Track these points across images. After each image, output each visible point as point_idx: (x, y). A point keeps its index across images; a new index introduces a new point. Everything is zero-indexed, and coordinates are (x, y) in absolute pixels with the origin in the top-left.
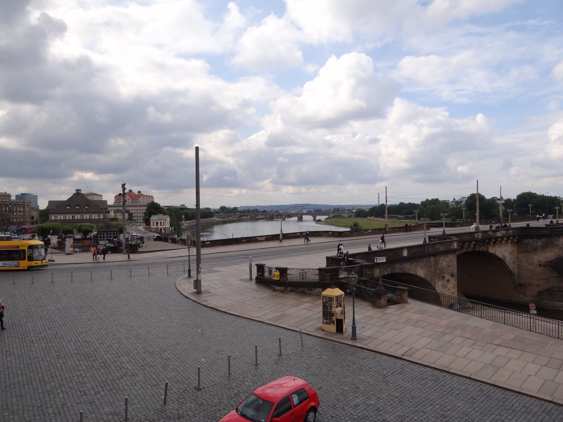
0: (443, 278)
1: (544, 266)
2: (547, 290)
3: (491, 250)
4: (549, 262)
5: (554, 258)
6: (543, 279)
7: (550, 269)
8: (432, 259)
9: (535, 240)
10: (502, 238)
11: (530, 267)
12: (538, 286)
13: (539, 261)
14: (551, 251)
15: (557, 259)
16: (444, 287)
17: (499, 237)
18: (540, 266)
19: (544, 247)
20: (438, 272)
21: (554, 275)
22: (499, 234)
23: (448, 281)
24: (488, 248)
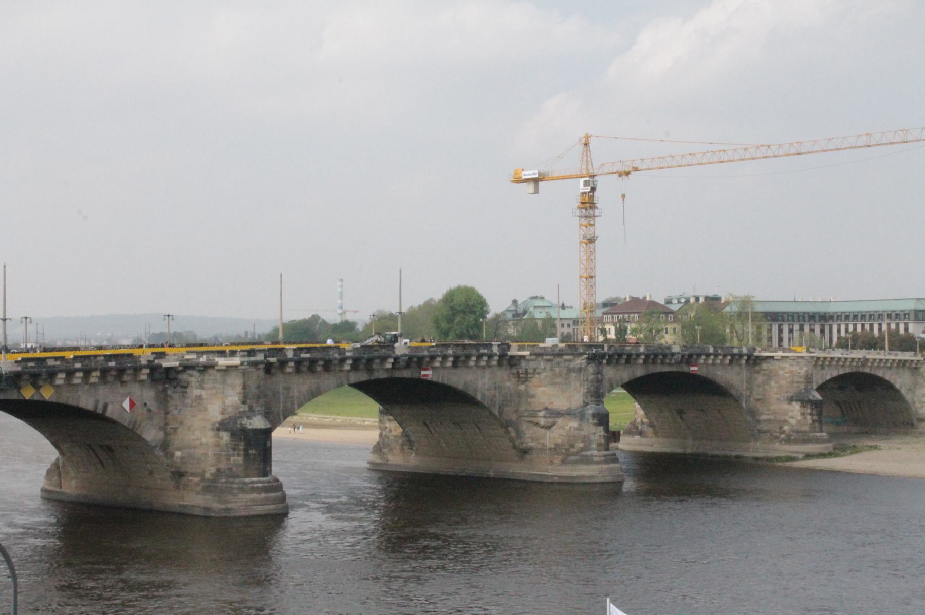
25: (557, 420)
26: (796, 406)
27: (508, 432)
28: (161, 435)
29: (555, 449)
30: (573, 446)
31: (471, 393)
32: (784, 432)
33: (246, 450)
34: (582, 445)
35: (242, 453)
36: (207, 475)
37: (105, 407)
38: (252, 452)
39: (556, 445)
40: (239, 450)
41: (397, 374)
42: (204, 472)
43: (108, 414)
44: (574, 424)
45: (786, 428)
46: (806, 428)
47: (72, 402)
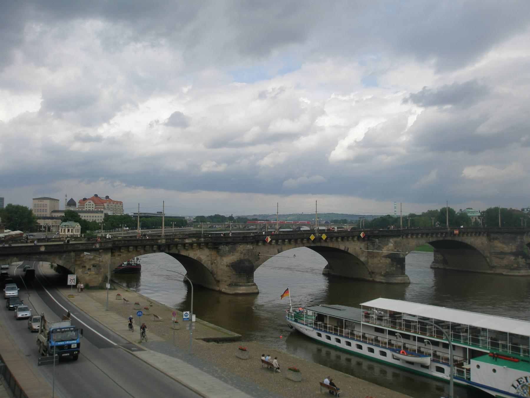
0: (85, 267)
1: (229, 266)
3: (184, 253)
8: (73, 254)
10: (191, 245)
11: (222, 267)
12: (226, 281)
15: (238, 261)
16: (83, 272)
17: (187, 243)
19: (229, 252)
20: (78, 262)
21: (234, 273)
22: (187, 241)
23: (89, 269)
24: (179, 251)
27: (486, 260)
28: (366, 259)
30: (512, 266)
31: (473, 245)
33: (397, 265)
34: (516, 265)
37: (348, 249)
38: (399, 266)
41: (446, 239)
43: (349, 251)
44: (512, 258)
47: (337, 247)
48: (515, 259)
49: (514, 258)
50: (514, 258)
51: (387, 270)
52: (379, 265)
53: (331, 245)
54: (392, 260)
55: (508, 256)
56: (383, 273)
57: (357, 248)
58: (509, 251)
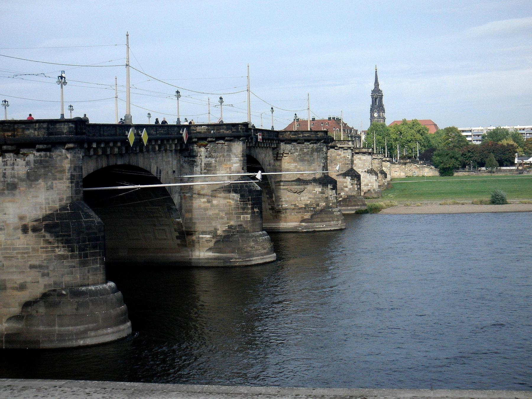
1: (35, 230)
2: (45, 296)
4: (47, 217)
5: (57, 206)
6: (32, 267)
7: (48, 235)
9: (10, 157)
12: (22, 287)
13: (21, 218)
14: (50, 188)
15: (63, 208)
18: (25, 229)
19: (32, 178)
21: (60, 252)
25: (306, 186)
26: (348, 179)
29: (305, 208)
30: (318, 205)
32: (341, 197)
33: (252, 208)
34: (324, 204)
35: (250, 211)
36: (219, 232)
39: (306, 205)
40: (248, 209)
42: (216, 230)
44: (318, 189)
45: (342, 194)
46: (354, 193)
47: (148, 169)
48: (322, 193)
49: (320, 190)
50: (320, 190)
51: (232, 223)
52: (210, 213)
53: (141, 162)
54: (242, 196)
55: (309, 187)
56: (219, 232)
57: (170, 172)
58: (311, 178)
